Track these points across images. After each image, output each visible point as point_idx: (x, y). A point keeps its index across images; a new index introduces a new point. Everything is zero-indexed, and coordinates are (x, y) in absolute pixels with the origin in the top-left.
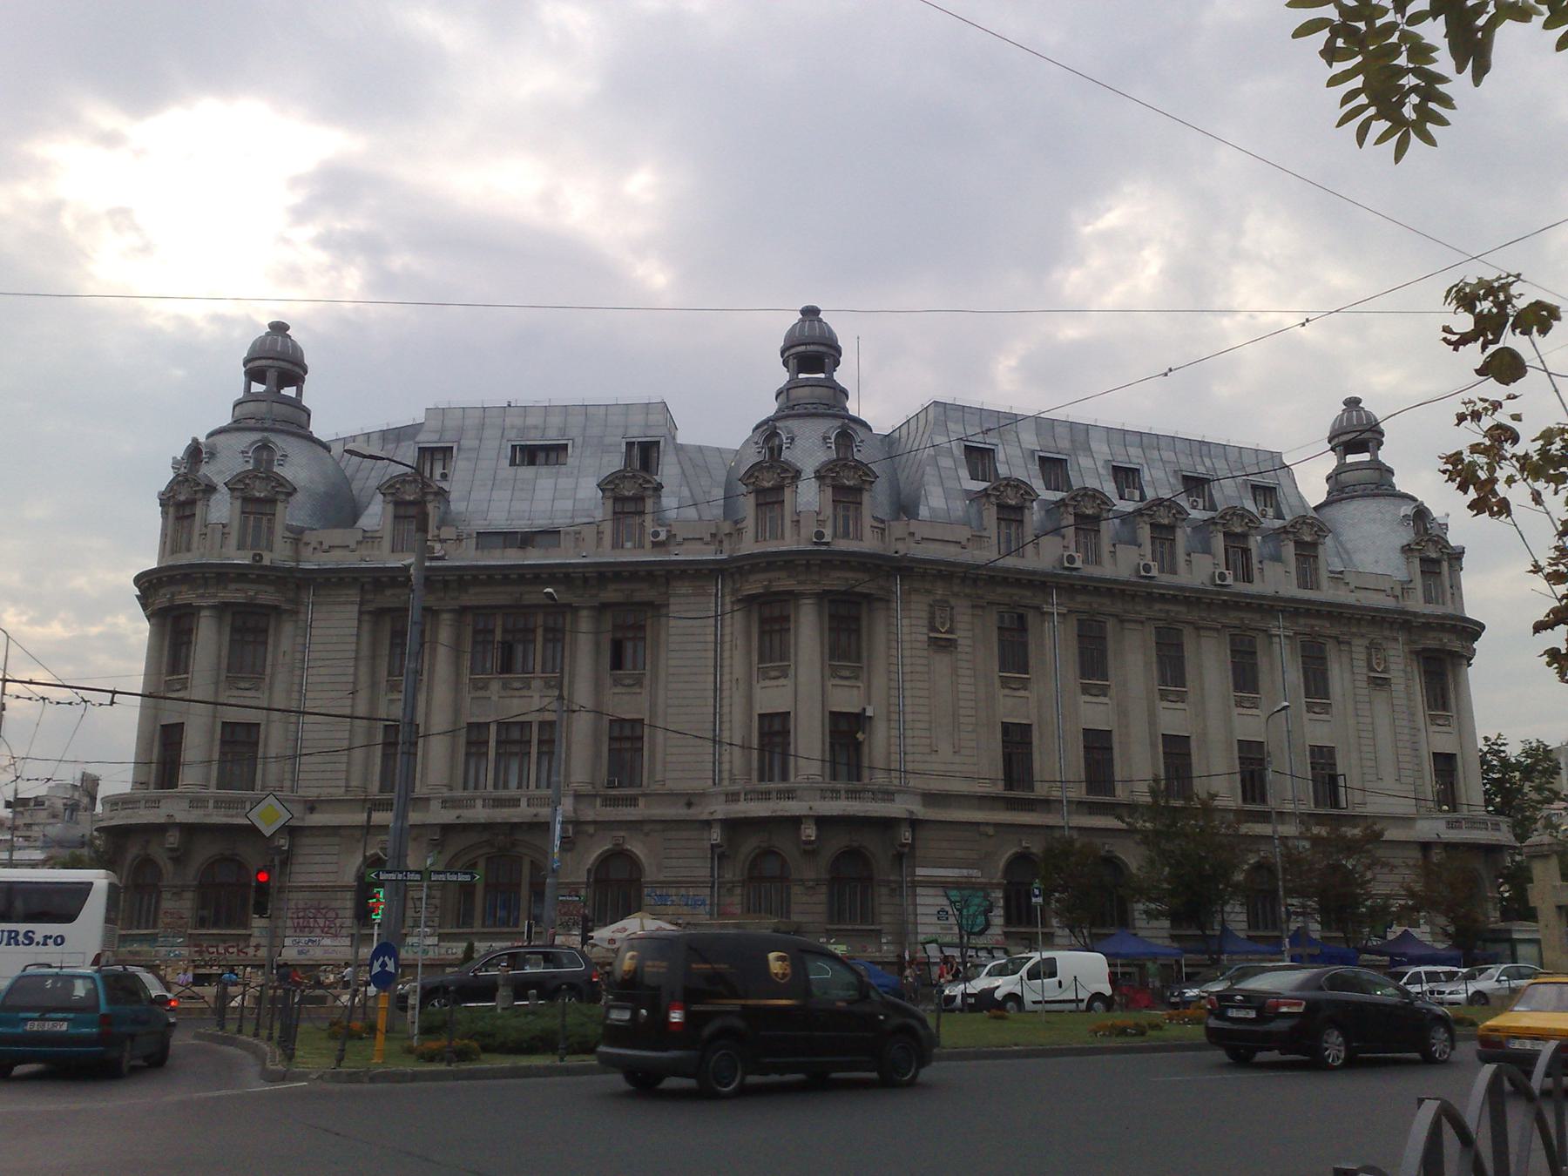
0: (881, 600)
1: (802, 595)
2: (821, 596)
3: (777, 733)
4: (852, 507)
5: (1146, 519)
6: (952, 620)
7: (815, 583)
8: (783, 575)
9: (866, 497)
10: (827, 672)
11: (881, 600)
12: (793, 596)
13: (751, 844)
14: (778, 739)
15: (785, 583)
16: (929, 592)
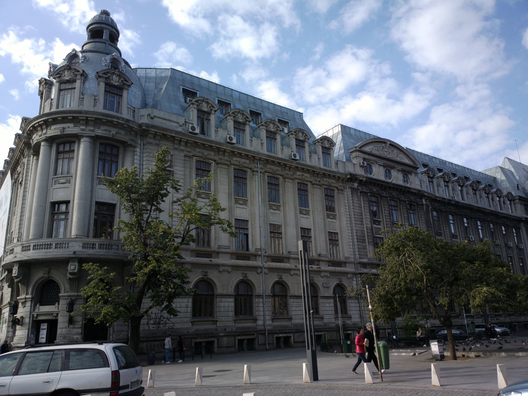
0: (131, 146)
1: (82, 136)
2: (95, 139)
3: (62, 213)
4: (116, 97)
5: (265, 127)
6: (171, 161)
7: (93, 131)
8: (71, 125)
9: (125, 93)
10: (96, 182)
11: (131, 146)
12: (77, 138)
13: (38, 276)
14: (63, 217)
15: (71, 129)
16: (158, 145)
